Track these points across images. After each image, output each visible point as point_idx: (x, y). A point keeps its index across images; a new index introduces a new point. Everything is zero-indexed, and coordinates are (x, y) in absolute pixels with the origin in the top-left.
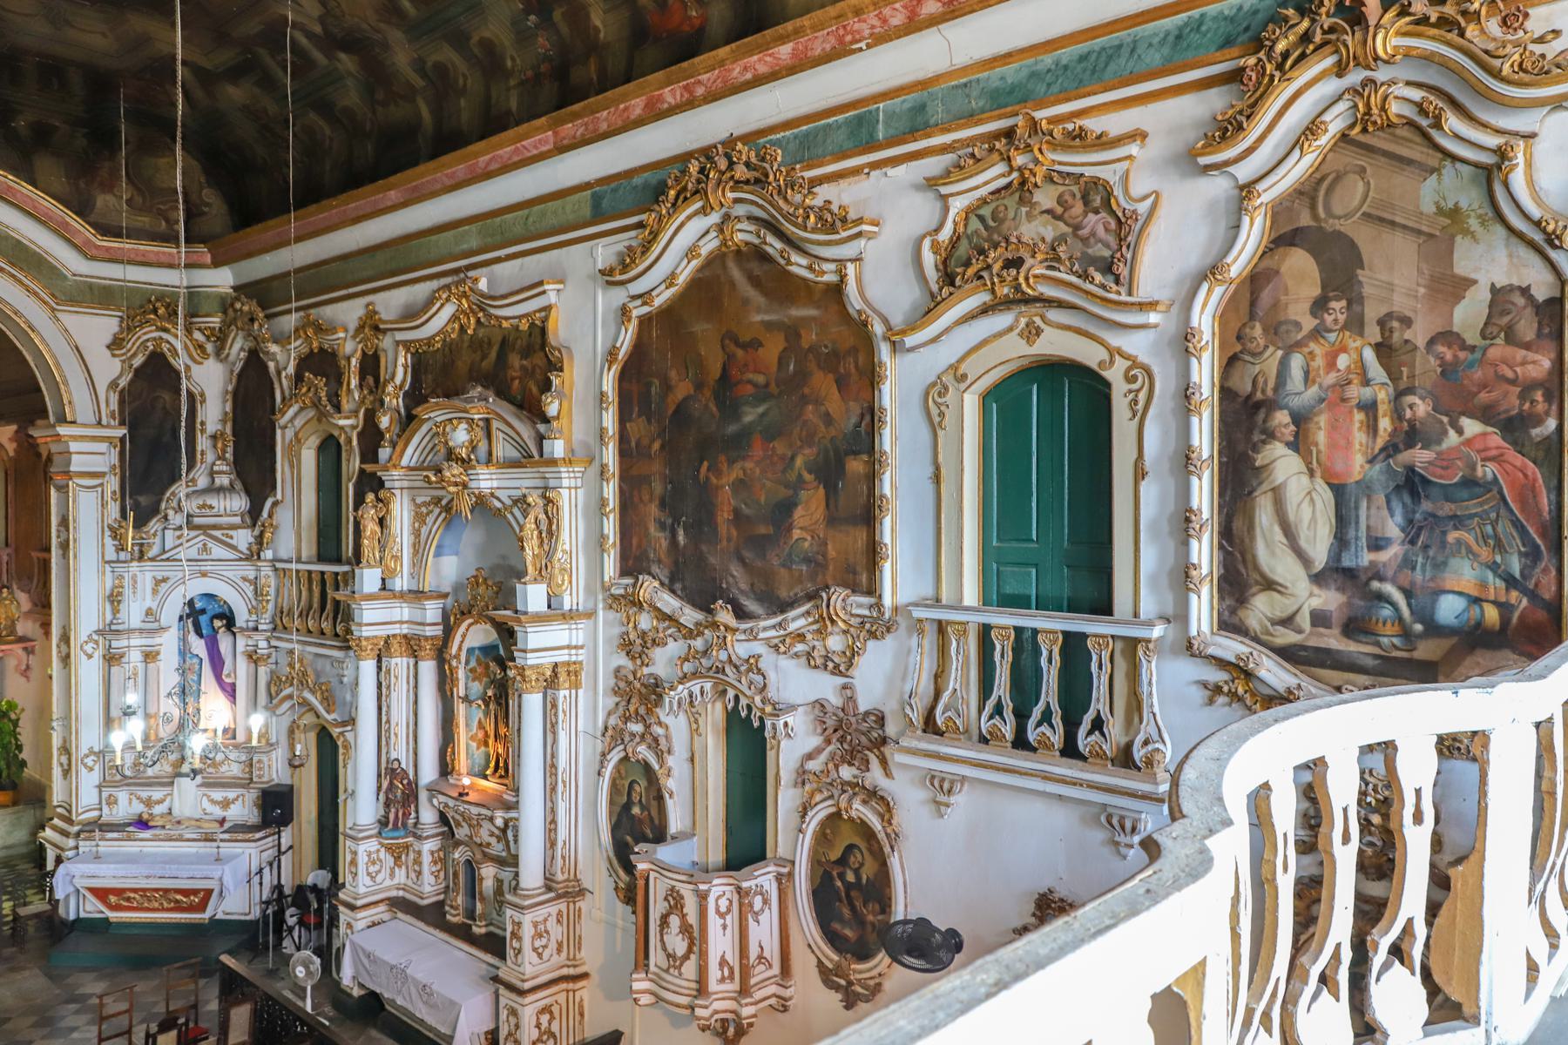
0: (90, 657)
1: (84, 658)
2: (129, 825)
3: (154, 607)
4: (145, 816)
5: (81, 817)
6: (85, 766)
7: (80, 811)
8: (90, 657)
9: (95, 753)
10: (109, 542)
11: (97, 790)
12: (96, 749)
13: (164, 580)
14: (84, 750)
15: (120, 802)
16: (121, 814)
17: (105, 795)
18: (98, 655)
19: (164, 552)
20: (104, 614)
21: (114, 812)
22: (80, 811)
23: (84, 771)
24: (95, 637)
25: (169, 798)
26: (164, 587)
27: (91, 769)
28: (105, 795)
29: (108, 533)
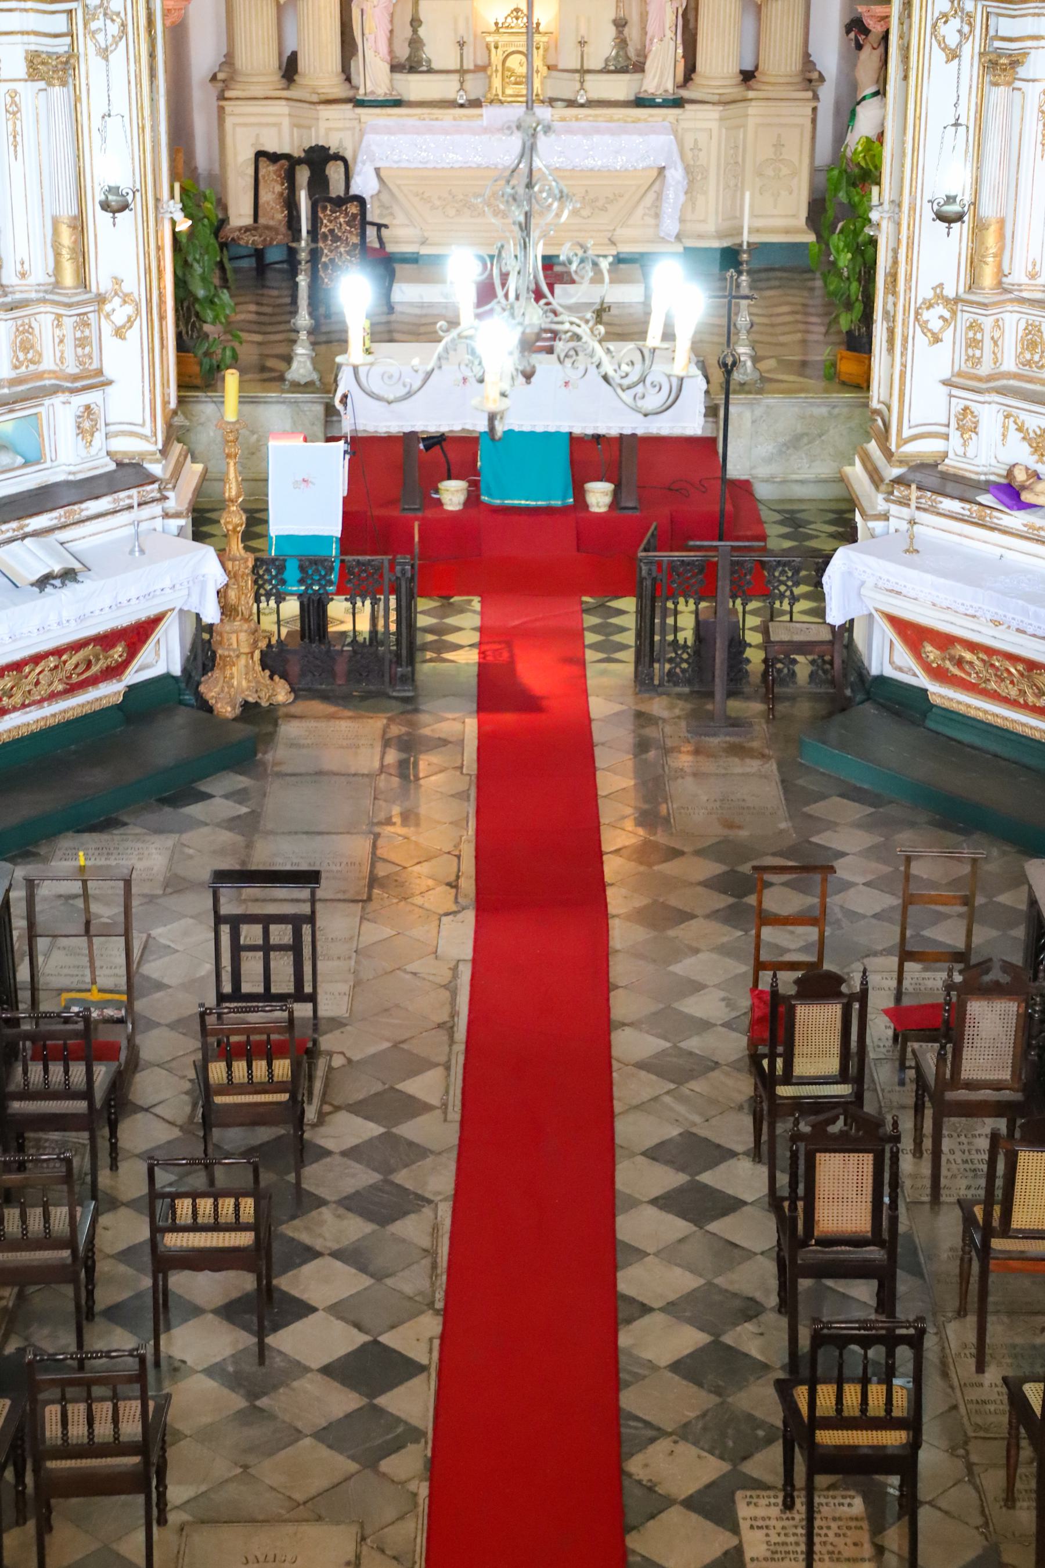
2: (988, 487)
4: (1020, 476)
5: (910, 448)
6: (924, 327)
9: (947, 301)
12: (950, 292)
14: (925, 292)
15: (982, 428)
16: (982, 460)
18: (970, 50)
21: (971, 451)
22: (906, 433)
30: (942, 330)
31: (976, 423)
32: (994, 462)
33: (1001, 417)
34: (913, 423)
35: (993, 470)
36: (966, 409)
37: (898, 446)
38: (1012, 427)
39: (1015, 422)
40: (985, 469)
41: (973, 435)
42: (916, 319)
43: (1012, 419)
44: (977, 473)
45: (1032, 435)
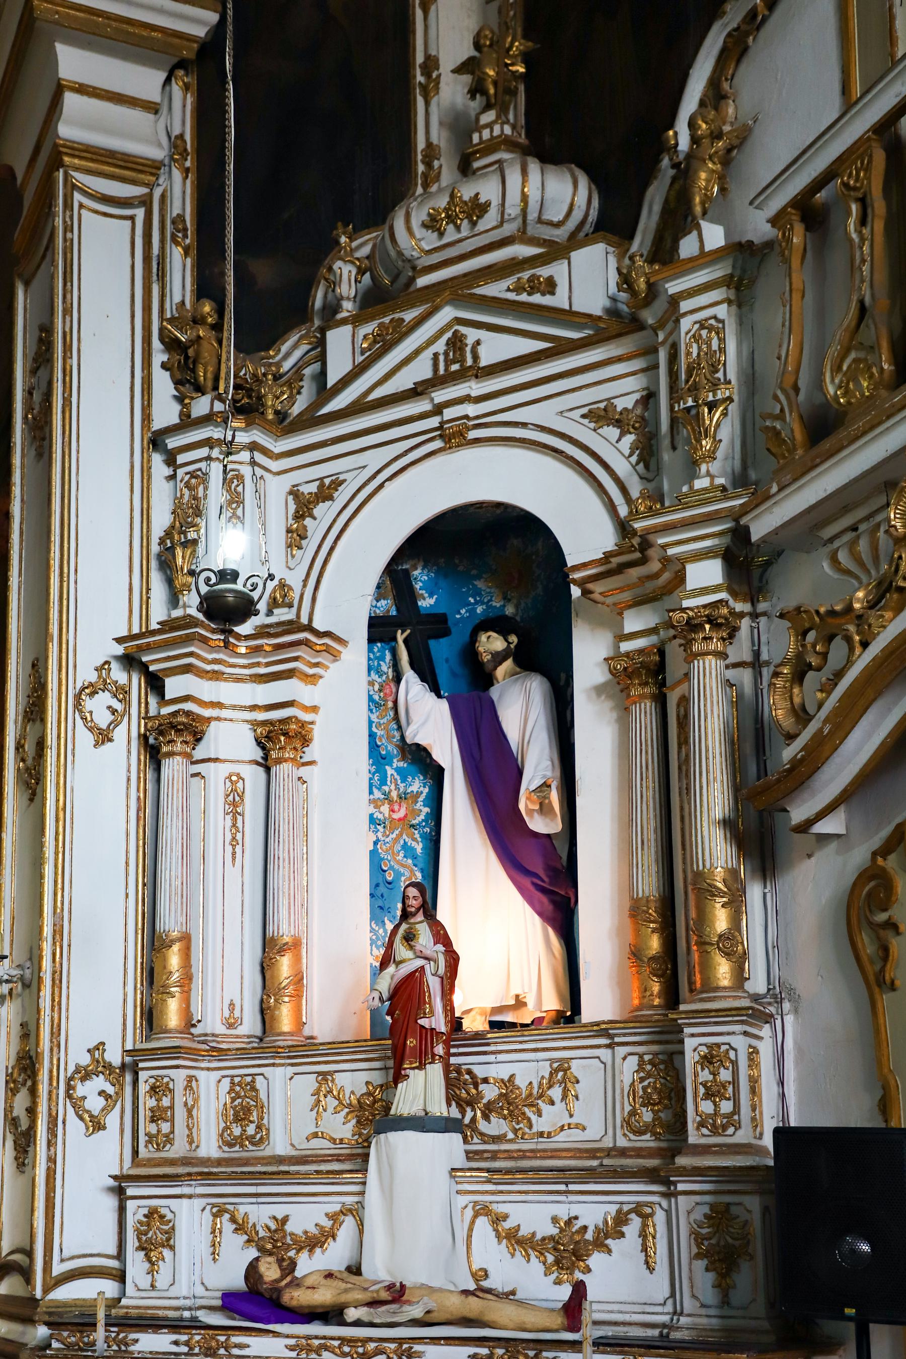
0: (103, 737)
1: (85, 738)
3: (294, 580)
5: (65, 1293)
7: (58, 1269)
8: (103, 737)
10: (163, 384)
11: (112, 1202)
13: (326, 492)
15: (181, 1239)
16: (183, 1288)
17: (135, 1211)
19: (324, 393)
20: (146, 602)
21: (162, 1280)
23: (74, 1127)
24: (119, 675)
25: (349, 1223)
26: (324, 512)
27: (97, 1125)
28: (135, 1211)
29: (159, 356)
30: (106, 1110)
31: (170, 1233)
32: (200, 1291)
33: (207, 1216)
34: (66, 1254)
35: (200, 1302)
36: (152, 1213)
37: (46, 1290)
38: (228, 1227)
39: (233, 1220)
40: (188, 1303)
41: (166, 1253)
42: (69, 1096)
43: (227, 1216)
44: (177, 1309)
45: (262, 1233)
